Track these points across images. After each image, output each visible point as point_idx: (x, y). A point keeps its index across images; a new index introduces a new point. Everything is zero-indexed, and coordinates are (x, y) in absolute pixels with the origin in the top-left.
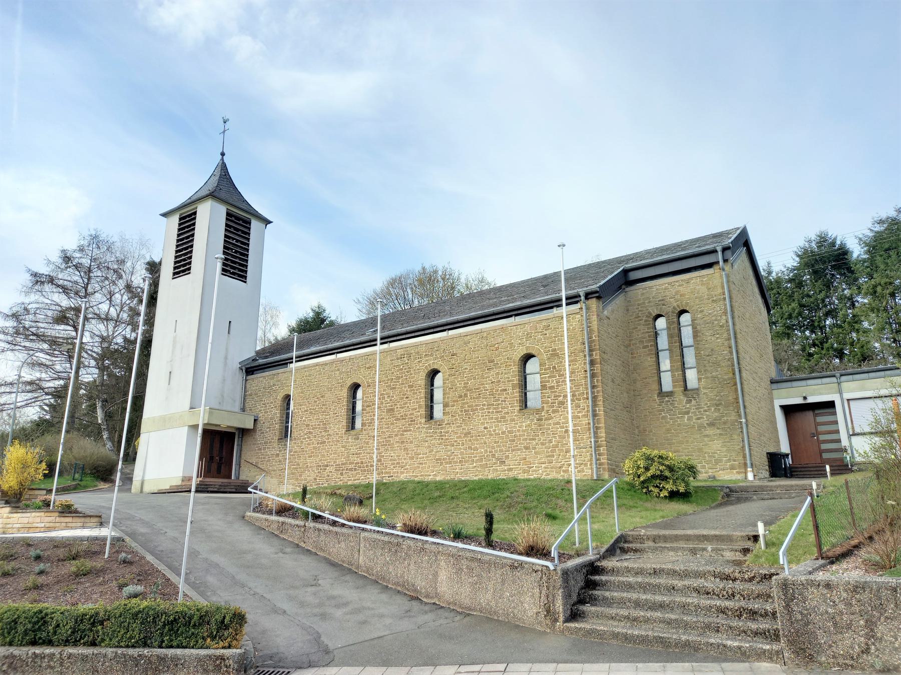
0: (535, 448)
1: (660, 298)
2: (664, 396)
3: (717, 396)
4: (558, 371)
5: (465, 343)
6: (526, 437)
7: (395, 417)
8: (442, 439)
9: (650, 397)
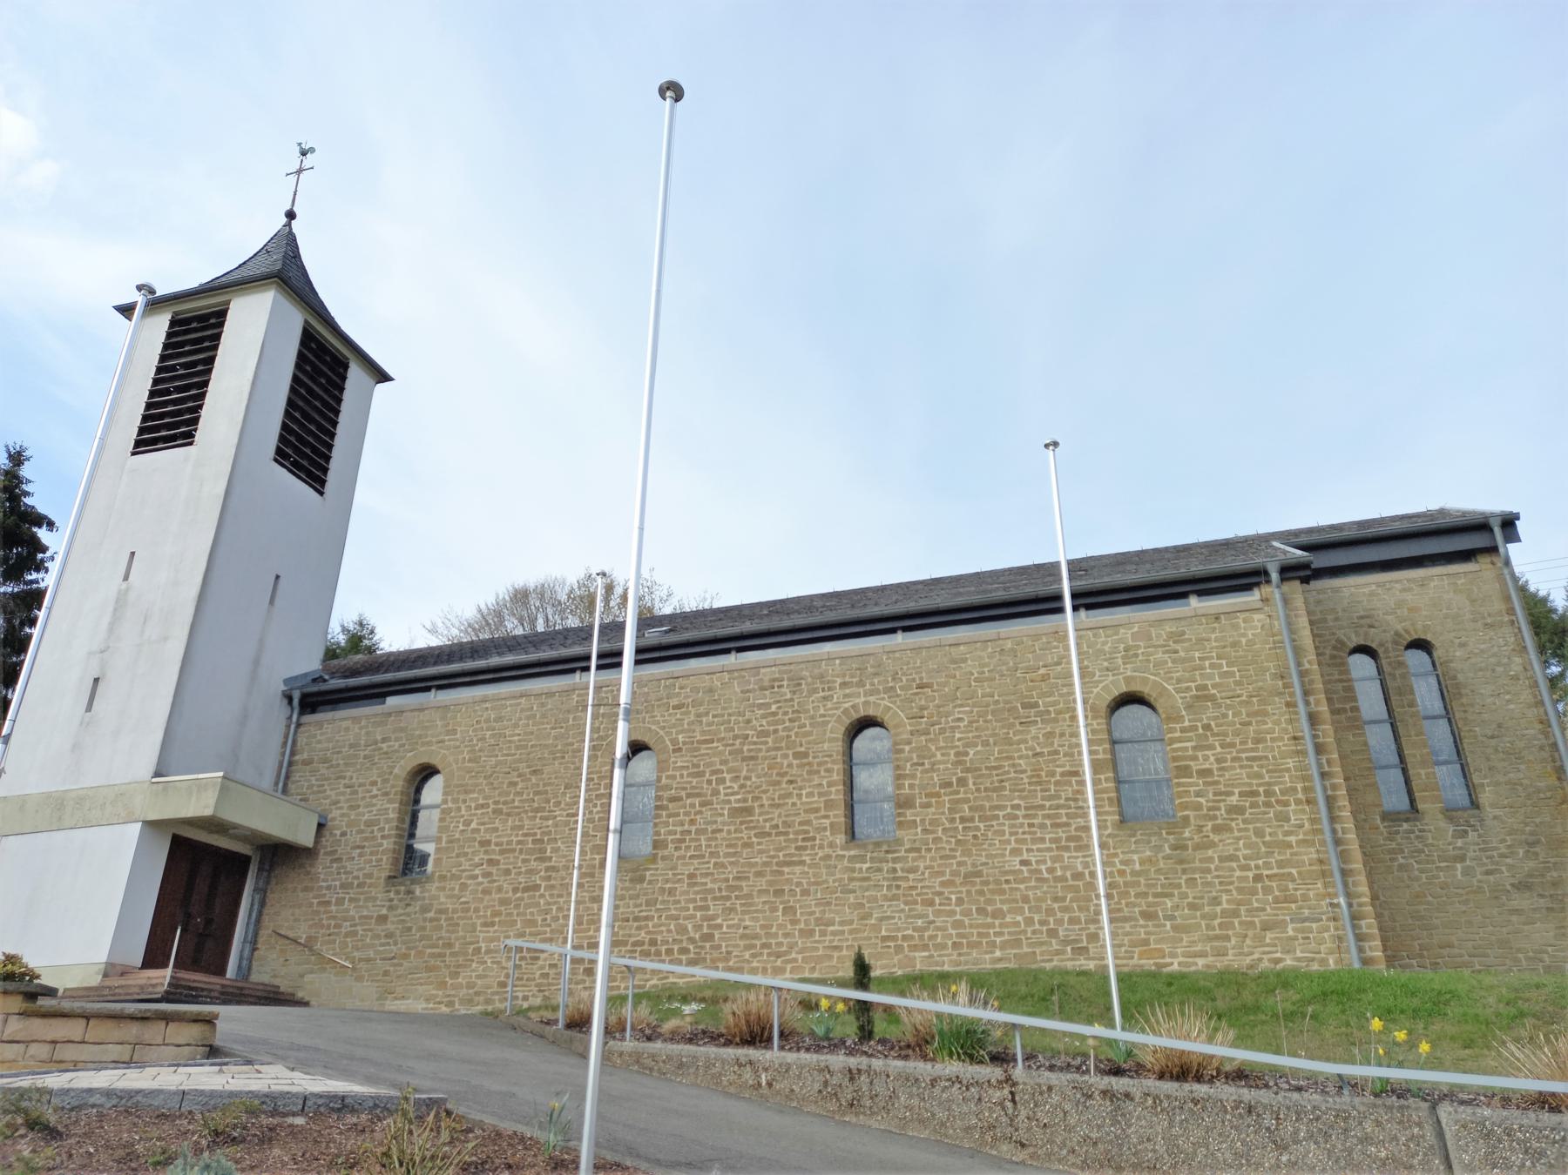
0: (1172, 918)
1: (1362, 613)
2: (1399, 820)
3: (1526, 824)
4: (1218, 735)
5: (954, 661)
6: (1143, 889)
7: (754, 828)
8: (898, 887)
9: (1365, 820)
